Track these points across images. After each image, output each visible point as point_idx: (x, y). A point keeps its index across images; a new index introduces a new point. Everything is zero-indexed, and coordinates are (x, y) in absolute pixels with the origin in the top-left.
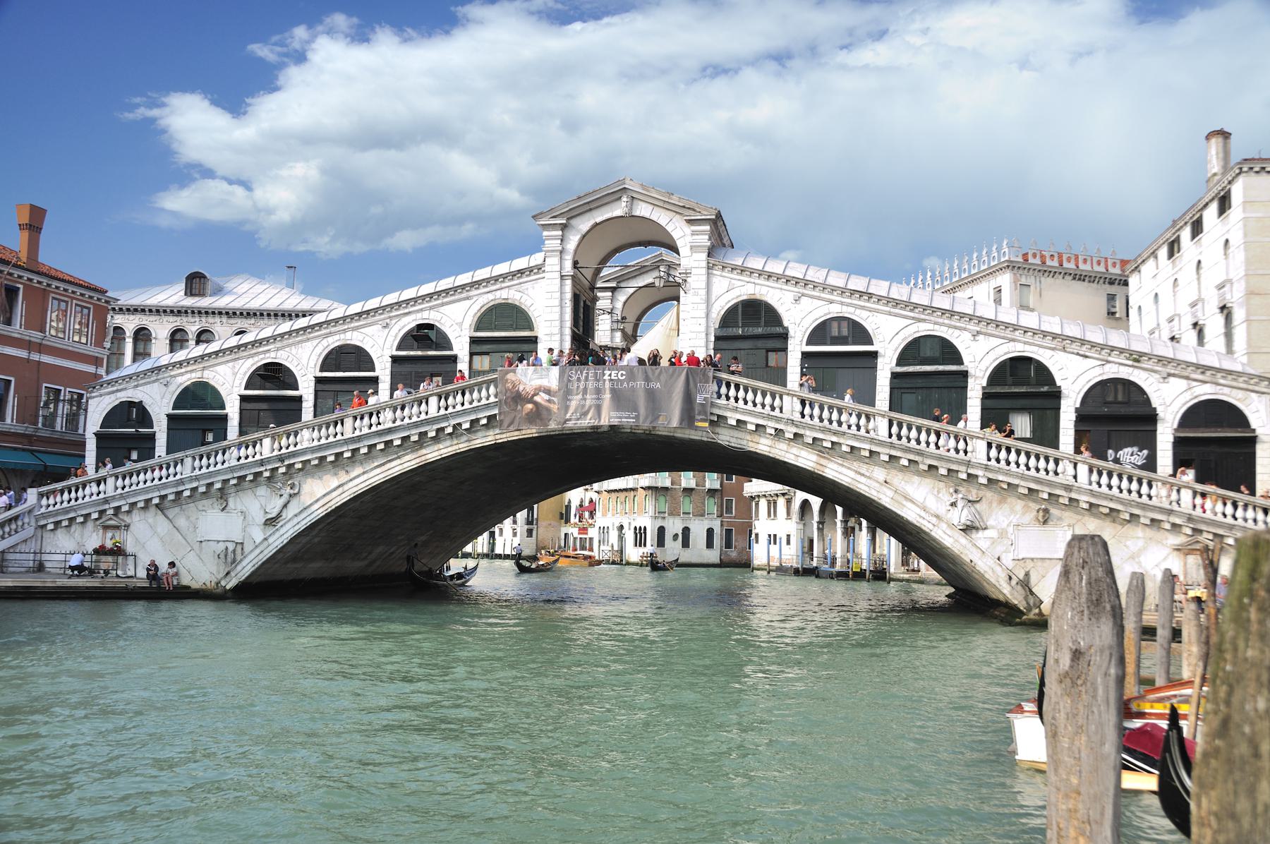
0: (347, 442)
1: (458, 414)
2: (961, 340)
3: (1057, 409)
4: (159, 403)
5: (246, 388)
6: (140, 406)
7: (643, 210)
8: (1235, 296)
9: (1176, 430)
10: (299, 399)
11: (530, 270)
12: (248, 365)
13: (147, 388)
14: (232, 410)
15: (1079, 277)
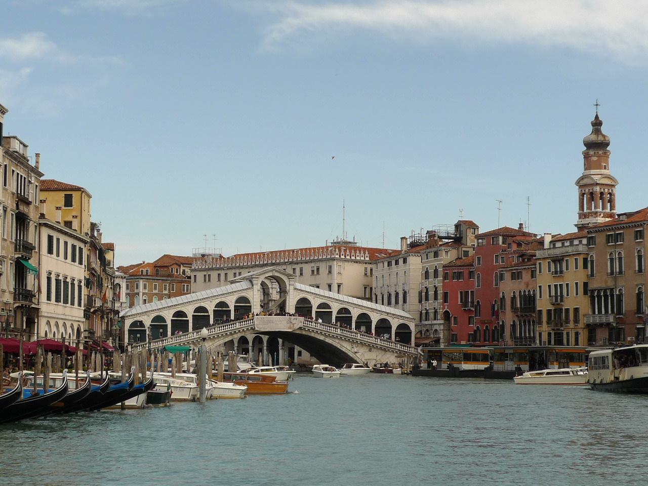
0: (216, 334)
1: (244, 327)
2: (351, 309)
3: (371, 326)
4: (147, 321)
5: (173, 317)
6: (141, 322)
7: (277, 274)
8: (407, 289)
9: (396, 330)
10: (188, 321)
11: (250, 288)
12: (173, 311)
13: (143, 317)
14: (169, 324)
15: (356, 262)
